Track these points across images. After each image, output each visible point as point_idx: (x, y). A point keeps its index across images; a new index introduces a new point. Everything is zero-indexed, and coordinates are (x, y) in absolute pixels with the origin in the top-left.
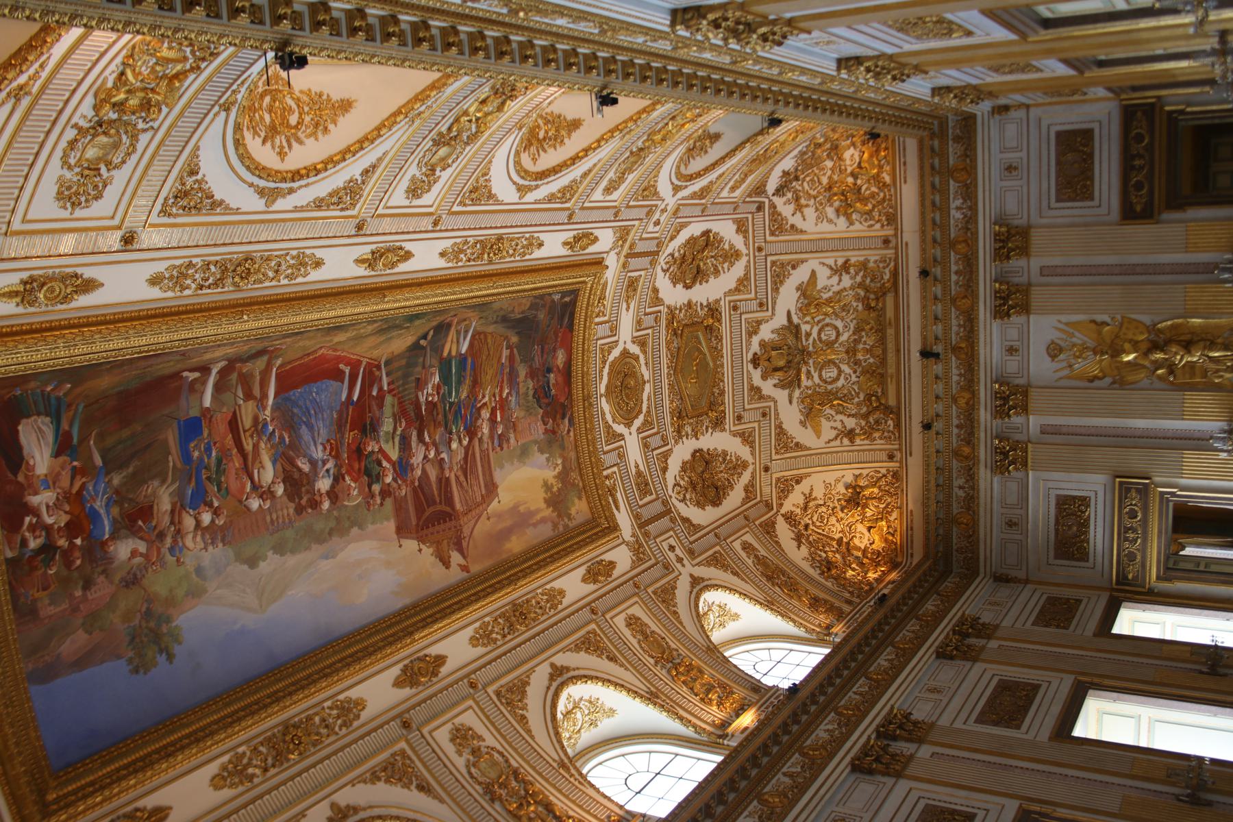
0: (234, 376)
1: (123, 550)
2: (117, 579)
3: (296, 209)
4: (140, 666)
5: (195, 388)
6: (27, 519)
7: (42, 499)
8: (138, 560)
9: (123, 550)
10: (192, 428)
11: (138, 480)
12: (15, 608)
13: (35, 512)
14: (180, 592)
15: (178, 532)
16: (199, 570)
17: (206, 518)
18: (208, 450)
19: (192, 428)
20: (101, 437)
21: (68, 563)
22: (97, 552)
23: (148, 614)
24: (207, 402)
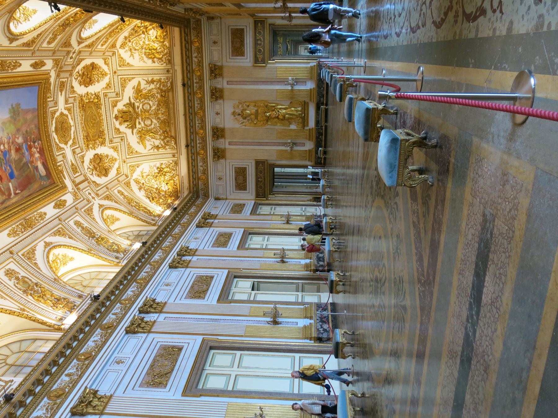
0: (7, 194)
1: (20, 140)
2: (21, 133)
3: (36, 245)
4: (18, 105)
5: (15, 188)
6: (38, 150)
7: (37, 155)
8: (17, 136)
9: (20, 140)
10: (12, 176)
11: (20, 160)
12: (39, 129)
13: (38, 152)
14: (8, 125)
15: (9, 143)
16: (3, 130)
17: (2, 147)
18: (5, 169)
19: (12, 176)
20: (30, 171)
21: (30, 138)
22: (26, 141)
23: (15, 120)
24: (10, 184)
